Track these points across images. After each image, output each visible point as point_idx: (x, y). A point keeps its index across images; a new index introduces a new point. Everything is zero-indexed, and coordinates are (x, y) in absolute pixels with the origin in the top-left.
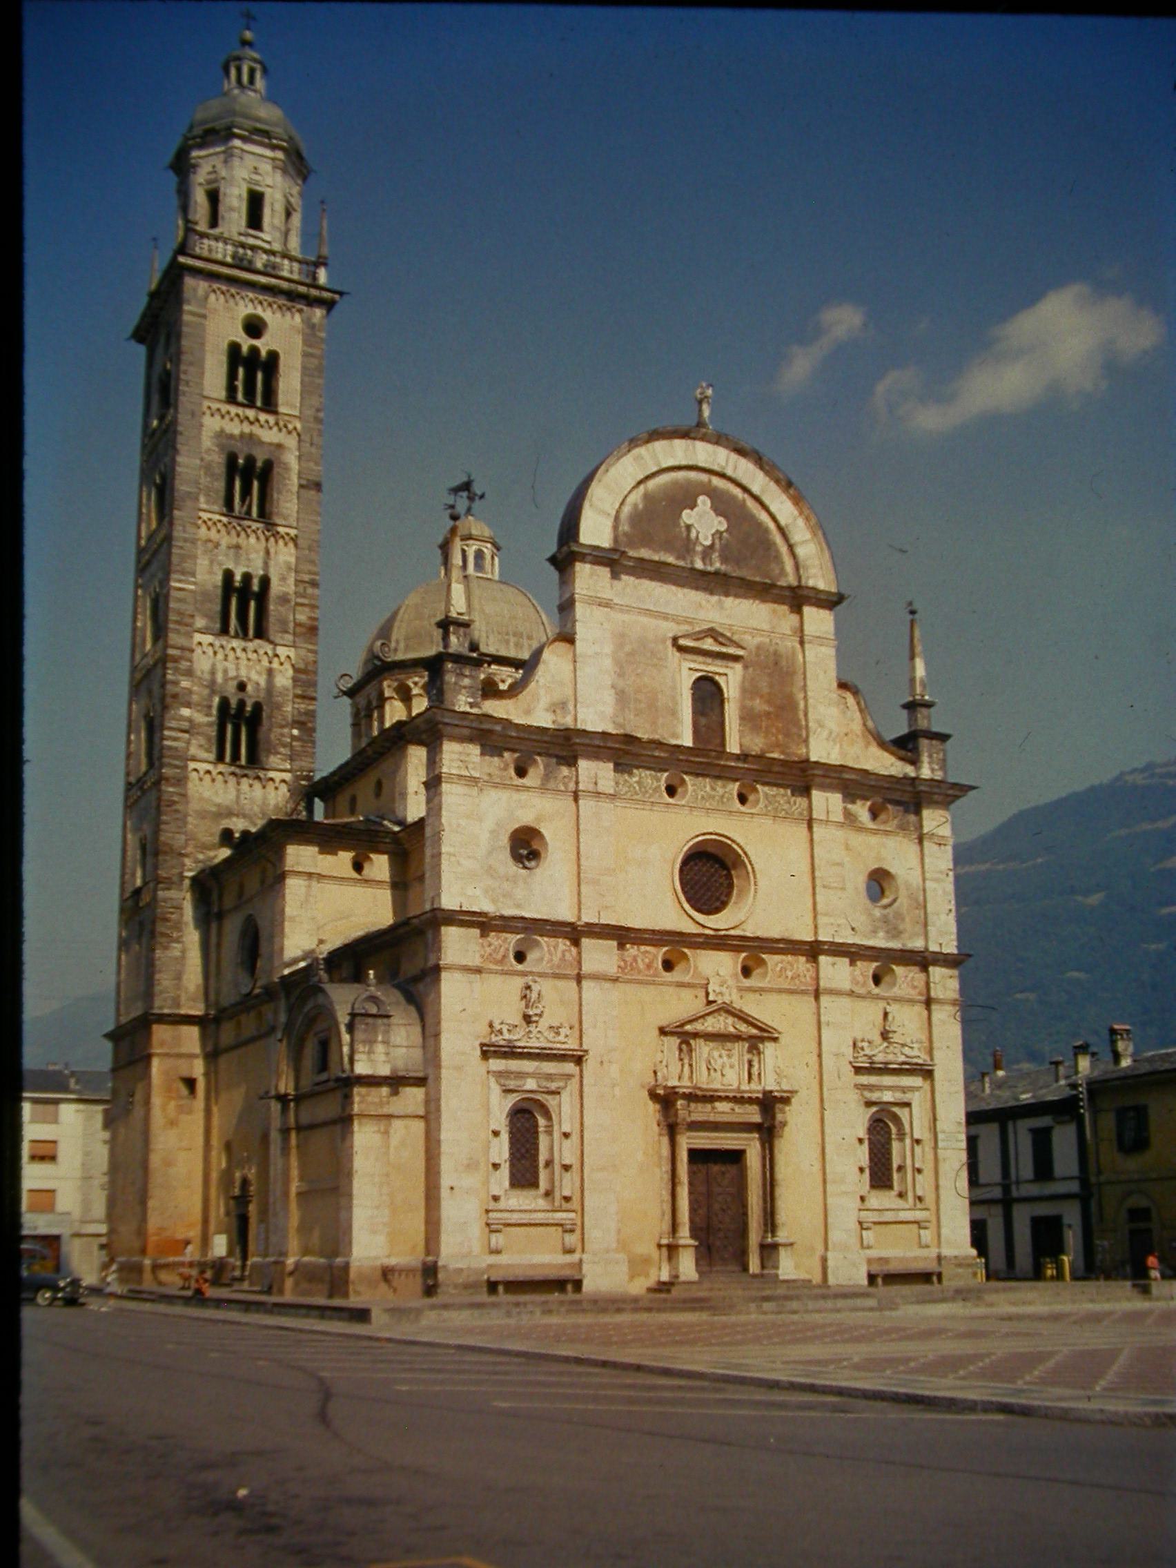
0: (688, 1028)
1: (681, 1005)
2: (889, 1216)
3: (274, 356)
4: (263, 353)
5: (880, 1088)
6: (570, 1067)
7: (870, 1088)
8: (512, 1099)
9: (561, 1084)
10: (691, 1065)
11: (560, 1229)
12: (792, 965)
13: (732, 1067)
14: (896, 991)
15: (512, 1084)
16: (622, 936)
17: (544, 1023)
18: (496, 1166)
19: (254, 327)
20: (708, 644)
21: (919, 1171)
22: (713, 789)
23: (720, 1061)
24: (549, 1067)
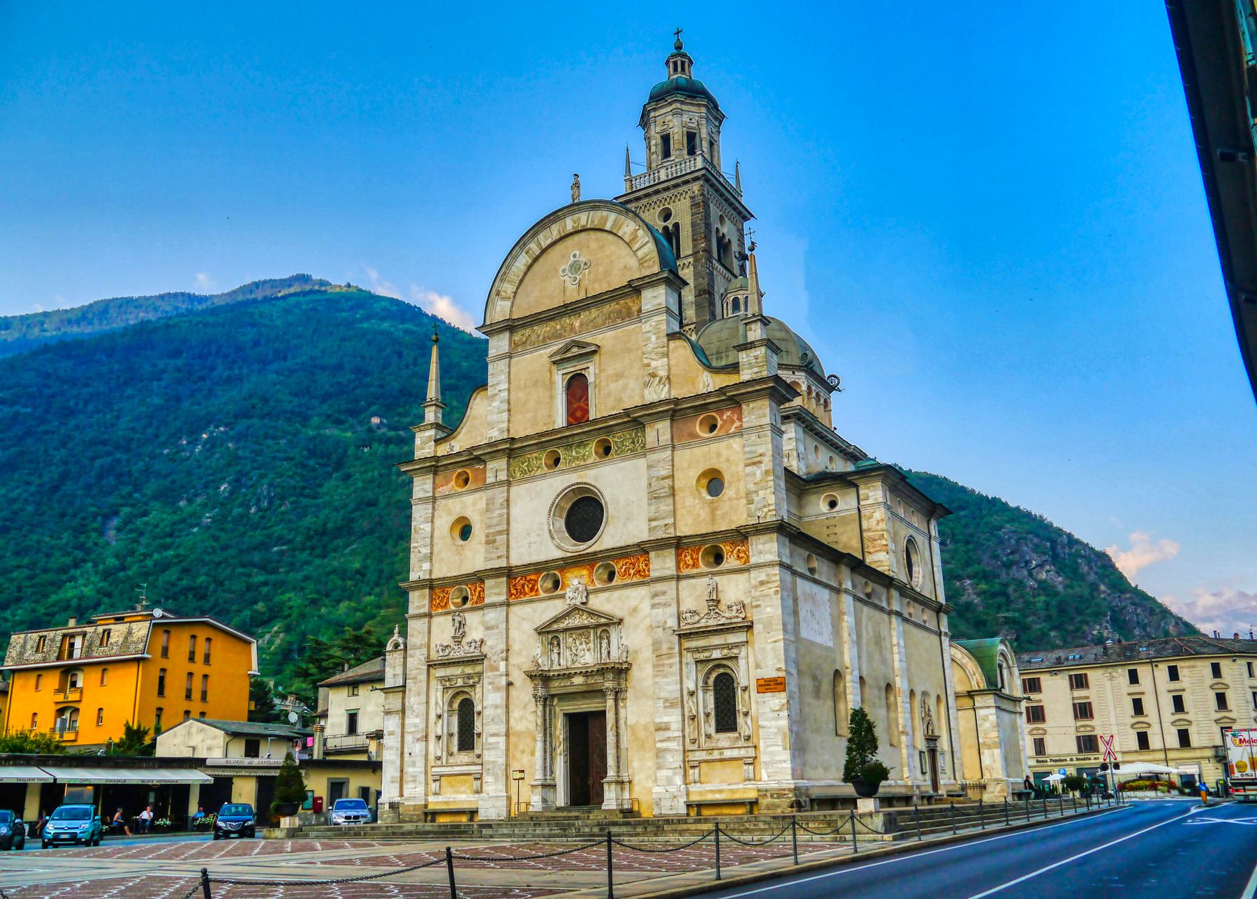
0: (555, 627)
1: (547, 610)
2: (716, 755)
3: (676, 226)
4: (670, 227)
5: (705, 649)
6: (478, 668)
7: (697, 650)
8: (451, 692)
9: (476, 680)
10: (559, 654)
11: (471, 778)
12: (633, 564)
13: (589, 650)
14: (724, 566)
15: (448, 684)
16: (509, 573)
17: (465, 641)
18: (439, 738)
19: (667, 215)
20: (575, 351)
21: (746, 714)
22: (577, 453)
23: (580, 647)
24: (469, 670)
